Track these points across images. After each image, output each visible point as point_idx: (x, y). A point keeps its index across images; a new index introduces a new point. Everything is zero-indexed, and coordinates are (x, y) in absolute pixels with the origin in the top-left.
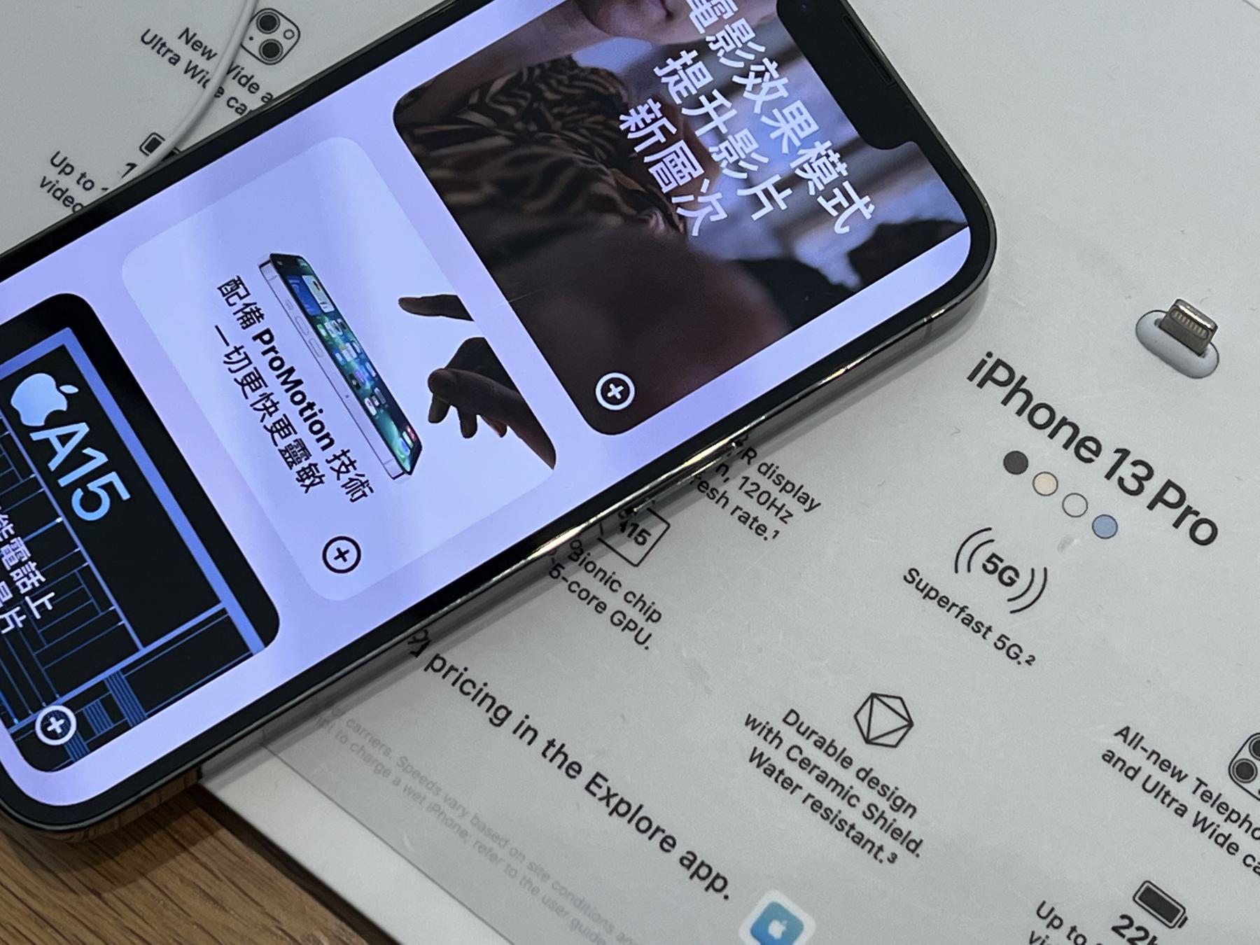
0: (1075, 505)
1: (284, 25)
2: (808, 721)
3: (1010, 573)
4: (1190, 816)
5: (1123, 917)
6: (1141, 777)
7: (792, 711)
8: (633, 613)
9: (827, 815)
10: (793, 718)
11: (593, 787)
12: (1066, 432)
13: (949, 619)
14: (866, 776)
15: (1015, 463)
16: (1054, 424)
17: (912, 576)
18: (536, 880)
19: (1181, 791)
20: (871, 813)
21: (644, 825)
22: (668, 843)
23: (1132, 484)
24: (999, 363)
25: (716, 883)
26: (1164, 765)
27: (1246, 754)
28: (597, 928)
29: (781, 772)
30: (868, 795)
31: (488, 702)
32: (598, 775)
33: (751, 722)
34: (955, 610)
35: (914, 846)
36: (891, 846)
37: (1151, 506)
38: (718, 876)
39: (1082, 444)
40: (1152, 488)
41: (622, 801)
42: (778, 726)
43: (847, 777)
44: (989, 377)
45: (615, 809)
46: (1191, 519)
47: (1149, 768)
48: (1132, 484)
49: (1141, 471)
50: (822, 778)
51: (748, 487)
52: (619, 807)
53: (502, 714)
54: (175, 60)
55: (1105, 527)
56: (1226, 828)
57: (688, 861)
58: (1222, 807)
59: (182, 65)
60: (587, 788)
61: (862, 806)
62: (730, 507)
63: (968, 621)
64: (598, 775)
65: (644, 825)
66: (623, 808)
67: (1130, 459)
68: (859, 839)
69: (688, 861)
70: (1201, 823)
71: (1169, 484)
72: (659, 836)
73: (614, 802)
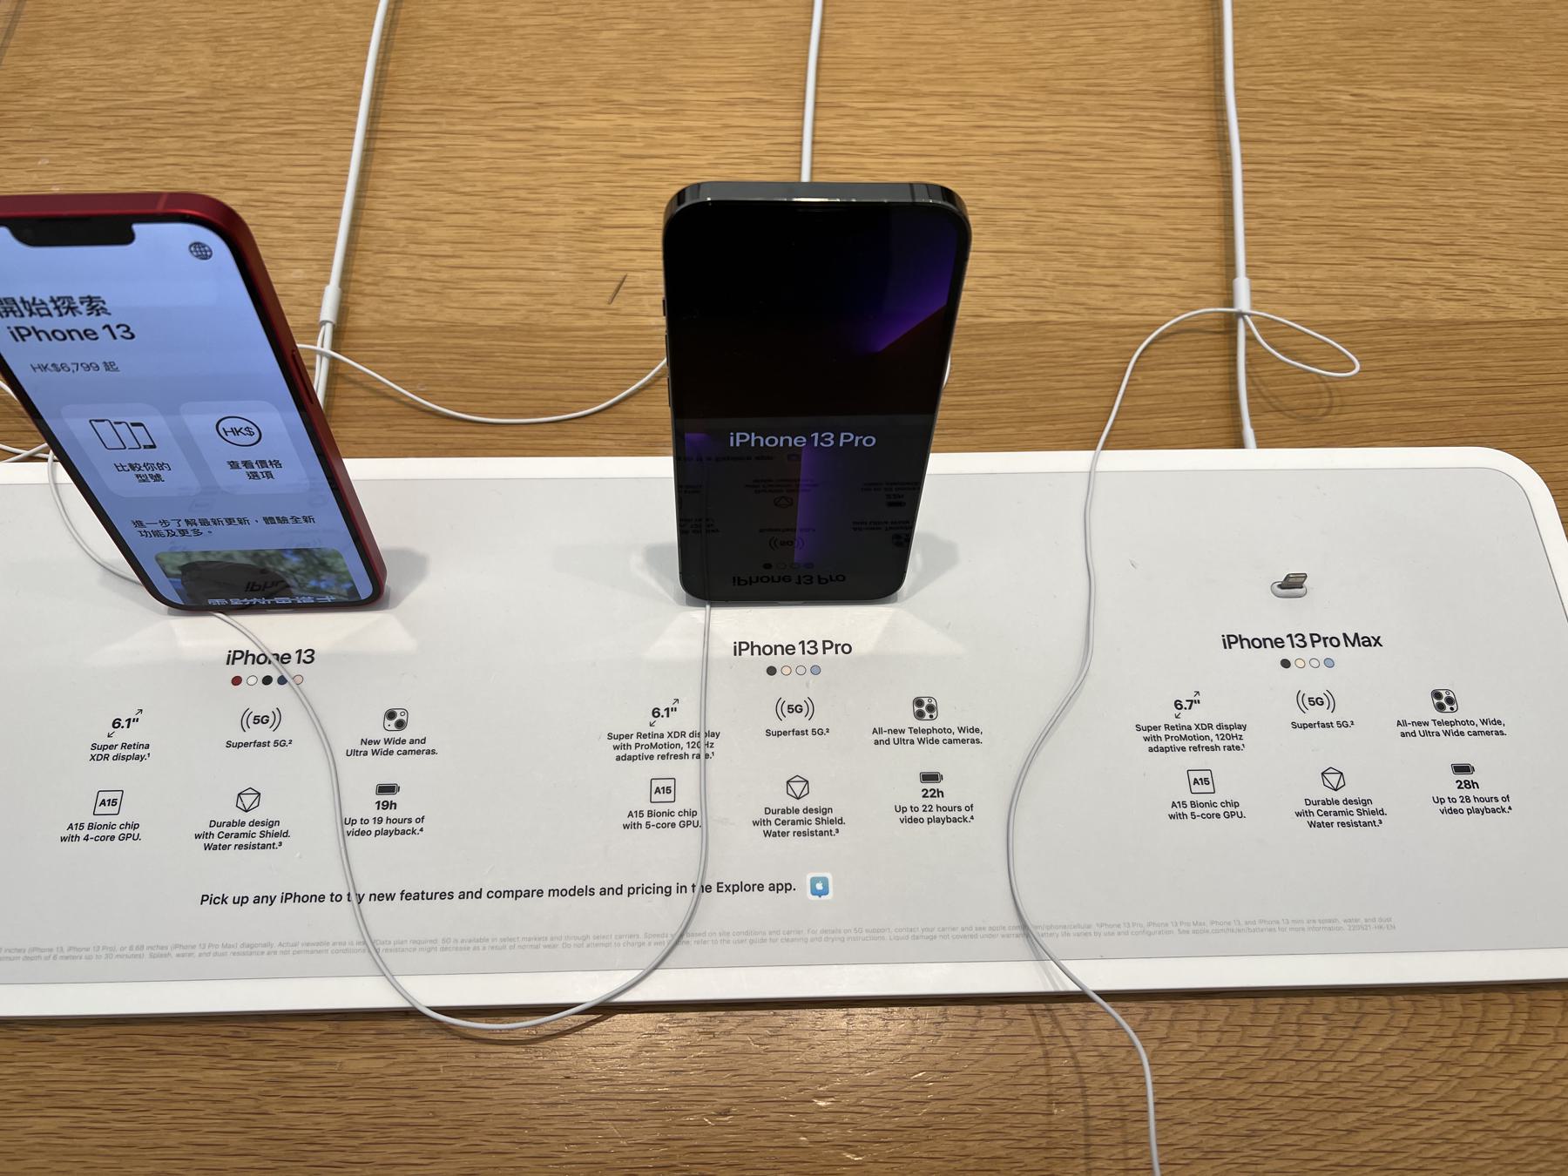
0: (801, 670)
1: (398, 712)
2: (773, 807)
3: (798, 708)
4: (916, 742)
5: (923, 791)
6: (891, 741)
7: (766, 808)
8: (686, 818)
9: (805, 834)
10: (768, 811)
11: (720, 889)
12: (779, 649)
13: (791, 737)
14: (808, 810)
15: (771, 671)
16: (774, 650)
17: (768, 733)
18: (725, 938)
19: (907, 735)
20: (818, 821)
21: (747, 888)
22: (760, 887)
23: (813, 650)
24: (740, 643)
25: (787, 887)
26: (895, 731)
27: (916, 709)
28: (760, 937)
29: (779, 832)
30: (813, 816)
31: (660, 889)
32: (718, 883)
33: (755, 823)
34: (791, 733)
35: (841, 821)
36: (833, 827)
37: (824, 653)
38: (786, 885)
39: (787, 649)
40: (820, 647)
41: (733, 886)
42: (765, 817)
43: (801, 816)
44: (741, 650)
45: (733, 890)
46: (839, 648)
47: (892, 736)
48: (813, 650)
49: (812, 644)
50: (793, 823)
51: (691, 745)
52: (734, 889)
53: (668, 890)
54: (366, 754)
55: (816, 670)
56: (930, 736)
57: (772, 887)
58: (923, 731)
59: (370, 753)
60: (718, 891)
61: (814, 822)
62: (690, 757)
63: (798, 733)
64: (718, 883)
65: (747, 888)
66: (736, 888)
67: (806, 643)
68: (822, 834)
69: (772, 887)
70: (921, 741)
71: (824, 642)
72: (756, 887)
73: (731, 888)
